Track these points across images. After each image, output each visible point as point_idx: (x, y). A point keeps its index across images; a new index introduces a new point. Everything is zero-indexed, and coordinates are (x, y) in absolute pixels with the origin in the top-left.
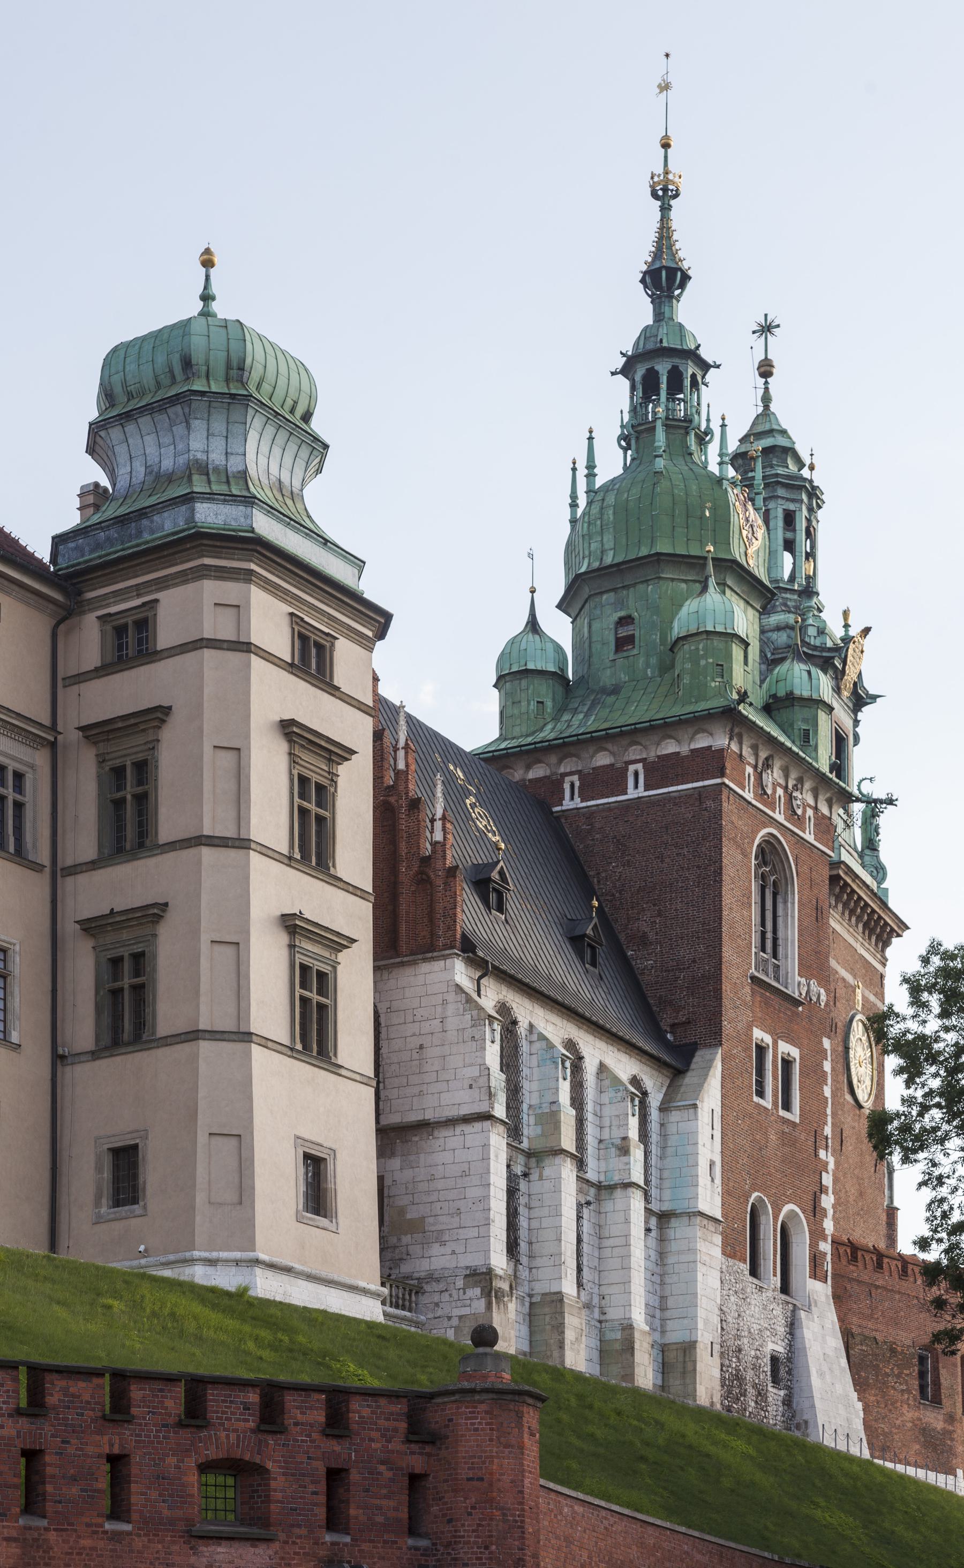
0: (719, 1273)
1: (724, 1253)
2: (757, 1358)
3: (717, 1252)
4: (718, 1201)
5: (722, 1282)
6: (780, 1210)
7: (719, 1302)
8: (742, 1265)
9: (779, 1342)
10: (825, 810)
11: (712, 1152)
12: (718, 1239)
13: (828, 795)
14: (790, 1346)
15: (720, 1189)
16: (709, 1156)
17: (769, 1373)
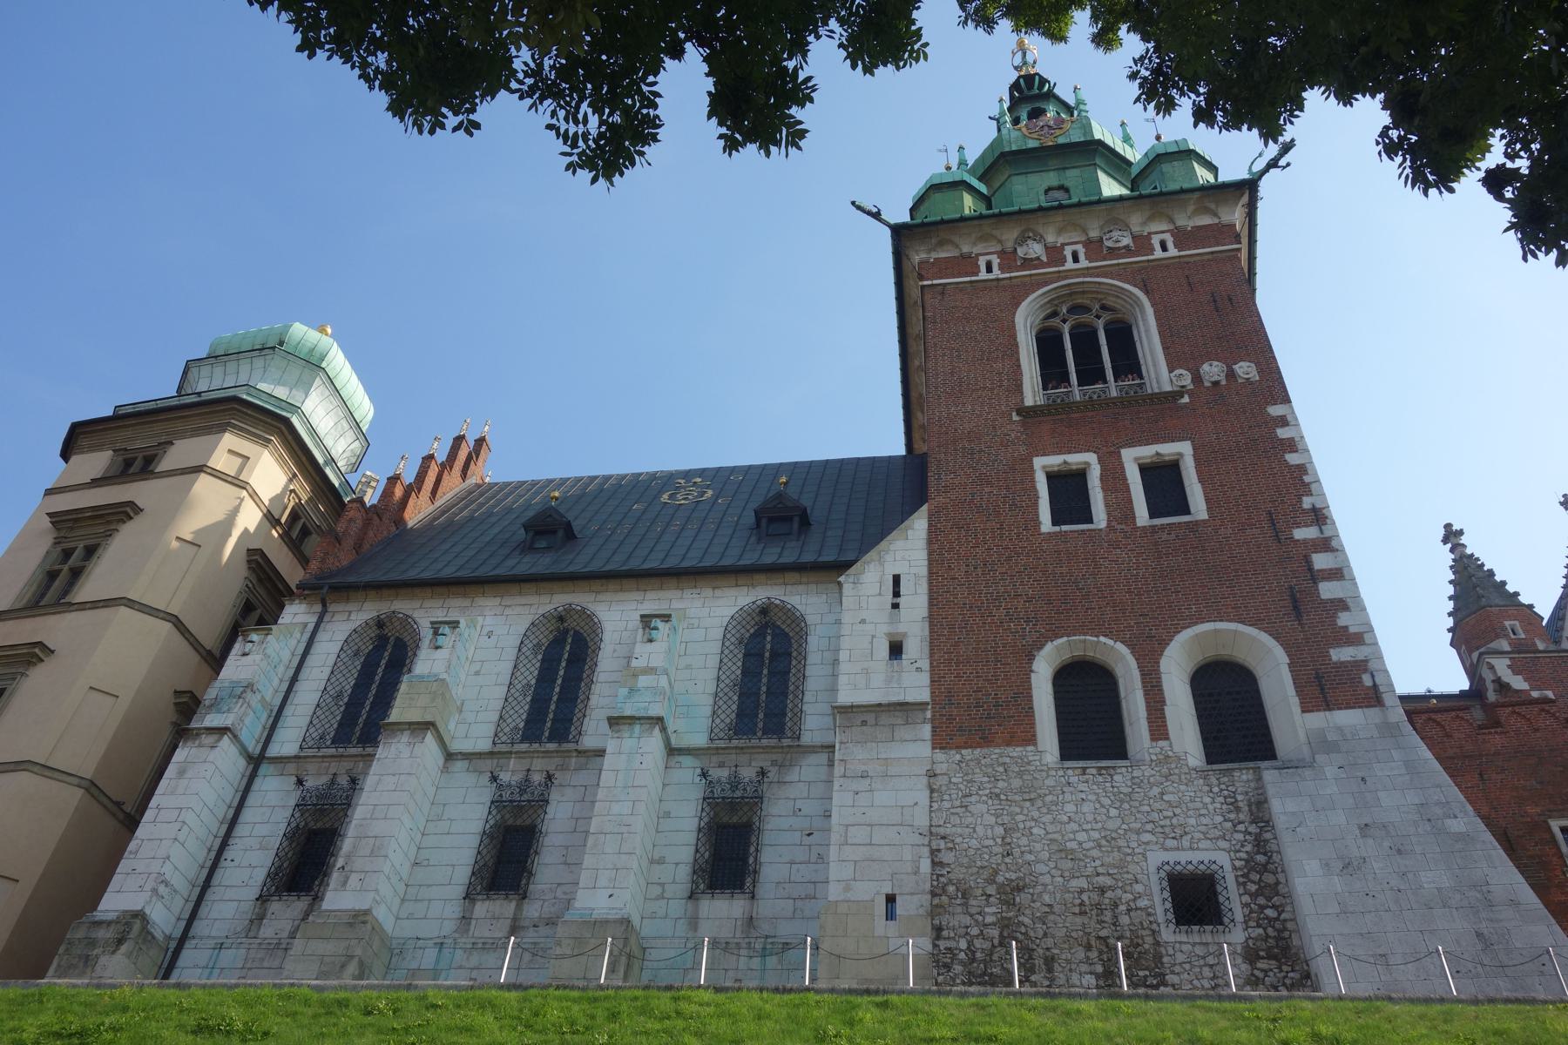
0: (925, 780)
1: (939, 743)
2: (1102, 890)
3: (925, 749)
4: (925, 679)
5: (932, 791)
6: (1164, 643)
7: (922, 820)
8: (1016, 751)
9: (1204, 844)
10: (1206, 220)
11: (893, 621)
12: (927, 730)
13: (1191, 208)
14: (1260, 844)
15: (925, 664)
16: (883, 629)
17: (1159, 910)
